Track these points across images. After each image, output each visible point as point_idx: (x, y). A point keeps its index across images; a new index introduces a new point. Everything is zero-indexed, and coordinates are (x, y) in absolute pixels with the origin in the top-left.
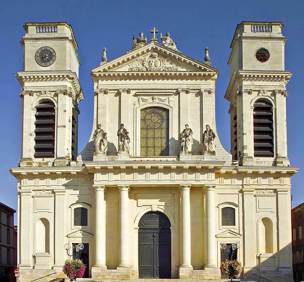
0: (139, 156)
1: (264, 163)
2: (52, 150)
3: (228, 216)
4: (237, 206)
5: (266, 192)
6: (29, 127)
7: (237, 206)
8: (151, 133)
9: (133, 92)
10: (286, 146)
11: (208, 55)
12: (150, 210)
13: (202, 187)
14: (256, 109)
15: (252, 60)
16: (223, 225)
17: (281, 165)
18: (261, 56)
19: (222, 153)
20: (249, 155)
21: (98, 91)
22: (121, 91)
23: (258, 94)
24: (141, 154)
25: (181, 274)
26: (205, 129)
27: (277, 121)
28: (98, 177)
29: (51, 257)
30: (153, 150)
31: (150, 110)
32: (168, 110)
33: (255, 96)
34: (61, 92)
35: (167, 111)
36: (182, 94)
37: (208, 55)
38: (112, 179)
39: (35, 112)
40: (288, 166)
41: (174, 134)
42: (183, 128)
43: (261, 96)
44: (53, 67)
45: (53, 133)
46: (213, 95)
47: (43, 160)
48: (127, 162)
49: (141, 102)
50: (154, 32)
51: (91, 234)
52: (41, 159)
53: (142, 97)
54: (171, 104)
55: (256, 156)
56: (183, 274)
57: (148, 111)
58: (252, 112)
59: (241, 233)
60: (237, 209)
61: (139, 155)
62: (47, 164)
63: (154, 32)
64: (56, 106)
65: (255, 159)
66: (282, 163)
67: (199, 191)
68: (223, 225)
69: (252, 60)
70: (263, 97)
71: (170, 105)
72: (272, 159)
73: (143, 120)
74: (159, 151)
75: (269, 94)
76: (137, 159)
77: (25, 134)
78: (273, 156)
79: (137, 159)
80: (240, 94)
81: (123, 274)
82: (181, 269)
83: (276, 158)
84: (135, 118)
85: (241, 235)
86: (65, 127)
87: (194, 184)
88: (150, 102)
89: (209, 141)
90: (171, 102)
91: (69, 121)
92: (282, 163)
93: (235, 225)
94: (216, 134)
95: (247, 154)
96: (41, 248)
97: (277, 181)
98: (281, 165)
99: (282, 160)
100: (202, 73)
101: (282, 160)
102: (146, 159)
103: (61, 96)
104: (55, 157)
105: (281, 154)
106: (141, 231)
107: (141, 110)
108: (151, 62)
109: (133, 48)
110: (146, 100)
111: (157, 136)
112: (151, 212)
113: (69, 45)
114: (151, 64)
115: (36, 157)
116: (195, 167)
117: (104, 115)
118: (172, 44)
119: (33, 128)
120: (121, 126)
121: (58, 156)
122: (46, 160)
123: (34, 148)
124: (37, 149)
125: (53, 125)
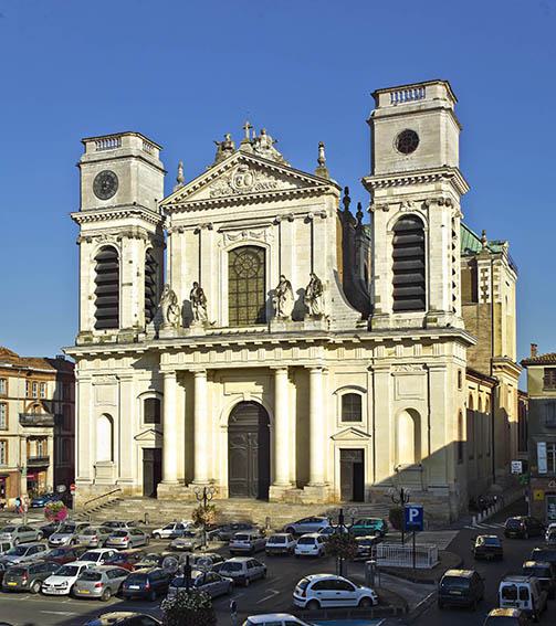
3: (352, 406)
4: (365, 391)
5: (411, 369)
6: (88, 289)
7: (365, 391)
9: (216, 227)
11: (322, 154)
12: (241, 399)
14: (397, 231)
17: (435, 324)
20: (383, 311)
21: (169, 230)
28: (166, 358)
32: (264, 250)
33: (394, 214)
35: (264, 250)
37: (322, 154)
38: (182, 361)
39: (95, 264)
41: (272, 283)
43: (404, 211)
44: (113, 201)
45: (117, 294)
51: (160, 434)
52: (103, 332)
55: (396, 310)
57: (238, 252)
58: (390, 238)
59: (371, 433)
60: (364, 396)
61: (226, 323)
62: (109, 338)
65: (393, 316)
66: (435, 320)
67: (300, 374)
72: (422, 315)
73: (232, 267)
74: (253, 313)
75: (418, 206)
77: (83, 298)
82: (271, 488)
86: (131, 284)
88: (240, 240)
90: (268, 237)
92: (435, 320)
96: (105, 455)
97: (428, 351)
98: (435, 324)
100: (309, 189)
103: (125, 240)
106: (232, 429)
112: (243, 402)
115: (97, 328)
117: (179, 264)
122: (109, 332)
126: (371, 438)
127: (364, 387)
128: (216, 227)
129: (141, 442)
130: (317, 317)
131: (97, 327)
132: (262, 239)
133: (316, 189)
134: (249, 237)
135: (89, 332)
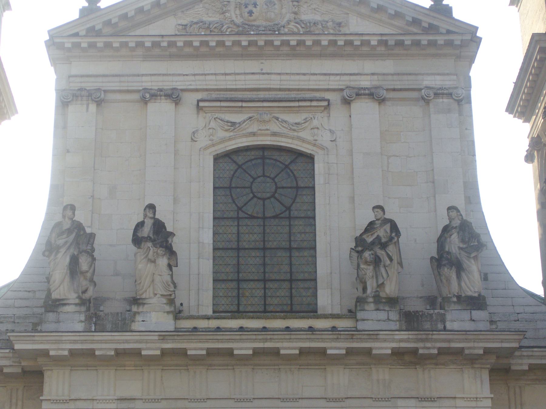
9: (191, 99)
22: (148, 96)
31: (252, 154)
32: (310, 158)
35: (310, 158)
48: (164, 336)
49: (221, 134)
53: (222, 116)
54: (324, 138)
57: (240, 159)
76: (202, 324)
79: (202, 324)
100: (424, 39)
102: (234, 324)
107: (217, 159)
108: (250, 7)
110: (233, 124)
114: (251, 13)
116: (414, 352)
128: (191, 99)
133: (440, 39)
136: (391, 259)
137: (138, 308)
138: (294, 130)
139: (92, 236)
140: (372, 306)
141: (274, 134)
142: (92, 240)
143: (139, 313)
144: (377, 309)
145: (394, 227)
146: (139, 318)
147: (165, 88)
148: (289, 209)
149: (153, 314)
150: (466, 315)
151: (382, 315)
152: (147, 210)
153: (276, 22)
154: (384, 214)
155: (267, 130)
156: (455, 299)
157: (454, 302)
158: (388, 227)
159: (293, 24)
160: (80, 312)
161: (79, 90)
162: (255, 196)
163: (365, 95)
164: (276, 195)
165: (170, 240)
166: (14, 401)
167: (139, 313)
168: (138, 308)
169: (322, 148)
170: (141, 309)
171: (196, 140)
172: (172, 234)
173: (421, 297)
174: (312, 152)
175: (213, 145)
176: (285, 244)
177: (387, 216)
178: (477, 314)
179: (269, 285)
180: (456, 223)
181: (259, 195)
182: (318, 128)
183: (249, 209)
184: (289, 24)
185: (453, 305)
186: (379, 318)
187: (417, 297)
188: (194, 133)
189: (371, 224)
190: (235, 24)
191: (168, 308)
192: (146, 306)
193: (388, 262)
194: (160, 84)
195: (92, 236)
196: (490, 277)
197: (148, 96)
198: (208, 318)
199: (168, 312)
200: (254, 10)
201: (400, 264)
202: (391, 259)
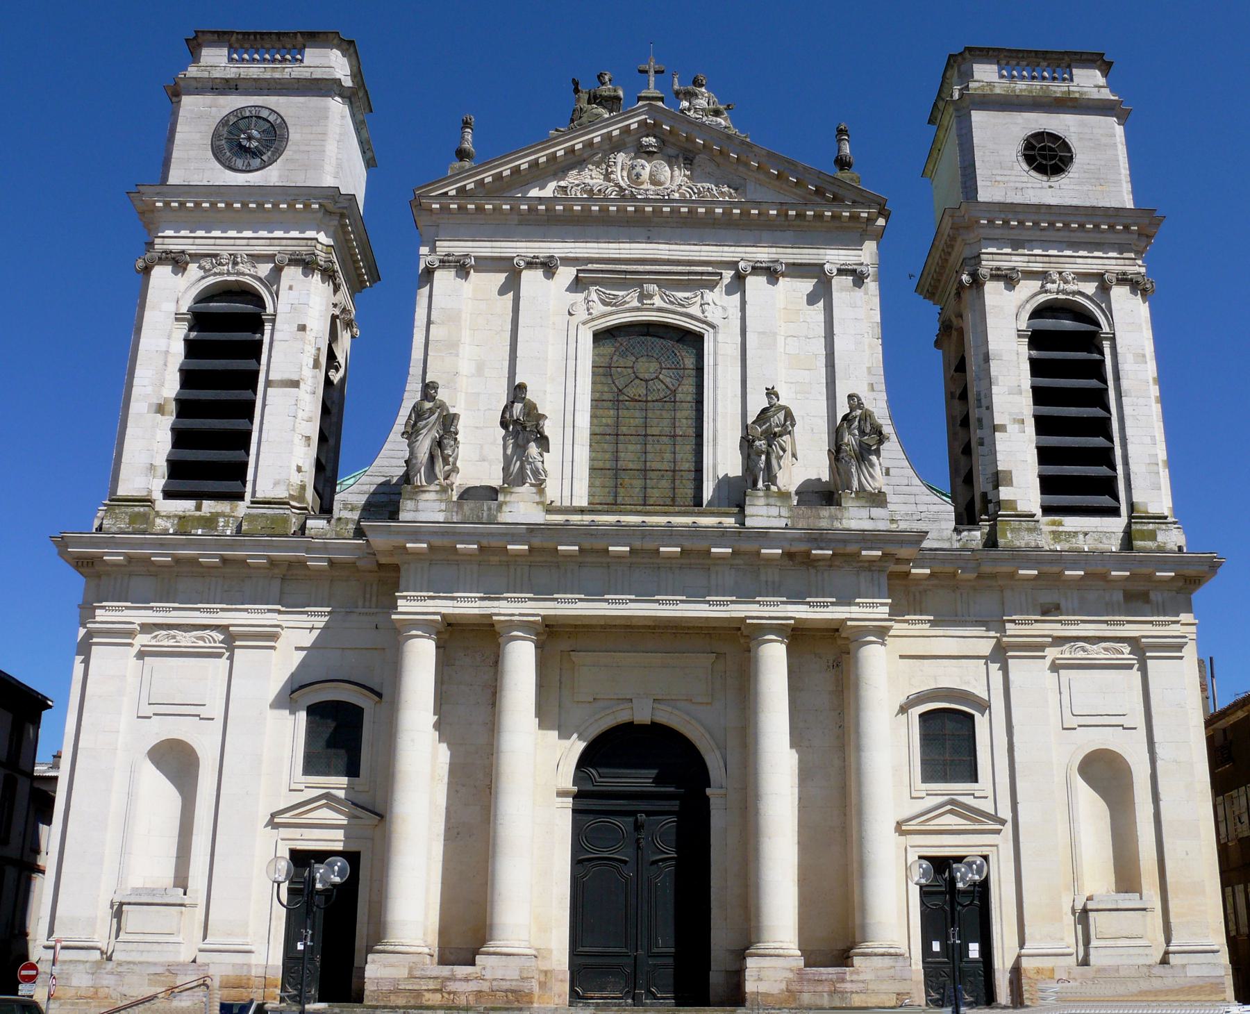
0: (584, 503)
1: (1081, 536)
2: (238, 471)
4: (984, 706)
8: (632, 419)
10: (1164, 475)
13: (837, 630)
14: (1037, 339)
15: (1012, 168)
16: (926, 779)
18: (1044, 157)
19: (912, 499)
20: (1022, 507)
22: (522, 263)
23: (1043, 286)
24: (591, 495)
25: (750, 987)
26: (843, 409)
27: (1125, 384)
29: (195, 906)
30: (638, 483)
34: (295, 261)
36: (755, 284)
39: (181, 332)
40: (1180, 548)
42: (757, 402)
43: (1054, 291)
44: (271, 176)
45: (246, 410)
46: (872, 286)
47: (198, 508)
50: (652, 73)
54: (713, 315)
55: (1047, 510)
56: (763, 988)
58: (1022, 352)
59: (1005, 813)
60: (981, 722)
61: (582, 500)
63: (652, 73)
64: (270, 309)
68: (926, 779)
69: (1012, 168)
70: (1061, 296)
71: (709, 319)
72: (1116, 525)
73: (602, 372)
77: (139, 406)
78: (1114, 512)
80: (977, 283)
81: (505, 985)
82: (751, 963)
83: (1130, 517)
84: (571, 363)
85: (1003, 822)
86: (295, 384)
87: (804, 616)
89: (864, 454)
91: (316, 364)
92: (1152, 536)
93: (976, 781)
94: (888, 429)
95: (1014, 502)
99: (1151, 527)
101: (1151, 527)
103: (291, 274)
104: (248, 496)
105: (1146, 504)
108: (638, 169)
109: (576, 121)
111: (655, 431)
113: (337, 108)
114: (638, 175)
115: (169, 494)
117: (453, 346)
118: (717, 113)
119: (172, 387)
120: (517, 391)
121: (260, 495)
122: (209, 506)
123: (168, 461)
124: (176, 469)
125: (250, 379)
126: (1009, 827)
127: (981, 692)
129: (284, 832)
130: (878, 499)
131: (169, 494)
132: (695, 310)
134: (657, 301)
135: (147, 501)
136: (784, 451)
137: (505, 497)
138: (683, 306)
139: (454, 417)
140: (762, 501)
141: (660, 310)
142: (455, 421)
143: (505, 503)
144: (768, 505)
145: (789, 415)
146: (505, 508)
147: (541, 255)
148: (674, 392)
149: (521, 504)
150: (864, 513)
151: (774, 511)
152: (518, 390)
153: (666, 186)
154: (778, 400)
155: (653, 304)
156: (853, 495)
157: (852, 498)
158: (781, 415)
159: (683, 188)
160: (441, 501)
161: (446, 255)
162: (637, 377)
163: (761, 268)
164: (661, 376)
165: (541, 422)
166: (368, 596)
167: (505, 503)
168: (505, 497)
169: (713, 326)
170: (508, 499)
171: (573, 313)
172: (543, 417)
173: (816, 492)
174: (701, 330)
175: (593, 320)
176: (667, 430)
177: (782, 402)
178: (876, 512)
179: (650, 474)
180: (859, 412)
181: (641, 376)
182: (709, 304)
183: (631, 391)
184: (680, 188)
185: (850, 501)
186: (770, 514)
187: (813, 492)
188: (572, 305)
189: (764, 411)
190: (620, 187)
191: (537, 498)
192: (513, 495)
193: (781, 453)
194: (537, 250)
195: (454, 417)
196: (892, 471)
197: (522, 263)
198: (582, 511)
199: (538, 503)
200: (642, 172)
201: (794, 455)
202: (784, 451)
